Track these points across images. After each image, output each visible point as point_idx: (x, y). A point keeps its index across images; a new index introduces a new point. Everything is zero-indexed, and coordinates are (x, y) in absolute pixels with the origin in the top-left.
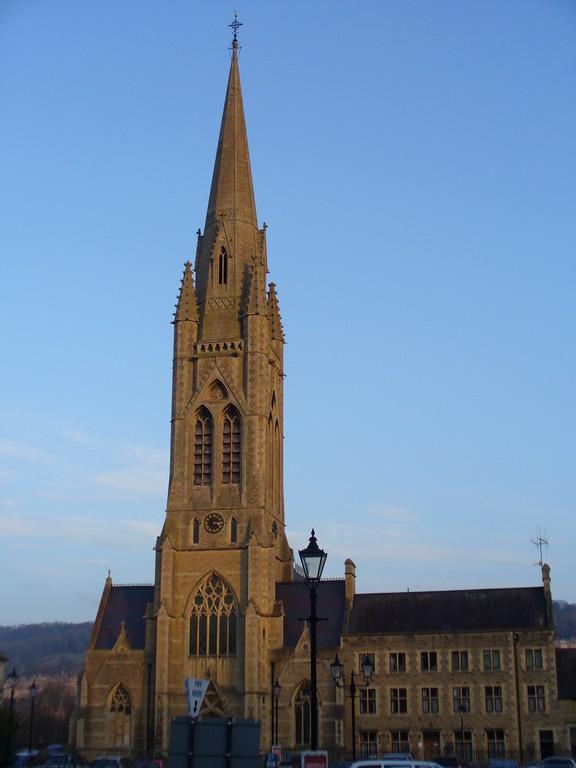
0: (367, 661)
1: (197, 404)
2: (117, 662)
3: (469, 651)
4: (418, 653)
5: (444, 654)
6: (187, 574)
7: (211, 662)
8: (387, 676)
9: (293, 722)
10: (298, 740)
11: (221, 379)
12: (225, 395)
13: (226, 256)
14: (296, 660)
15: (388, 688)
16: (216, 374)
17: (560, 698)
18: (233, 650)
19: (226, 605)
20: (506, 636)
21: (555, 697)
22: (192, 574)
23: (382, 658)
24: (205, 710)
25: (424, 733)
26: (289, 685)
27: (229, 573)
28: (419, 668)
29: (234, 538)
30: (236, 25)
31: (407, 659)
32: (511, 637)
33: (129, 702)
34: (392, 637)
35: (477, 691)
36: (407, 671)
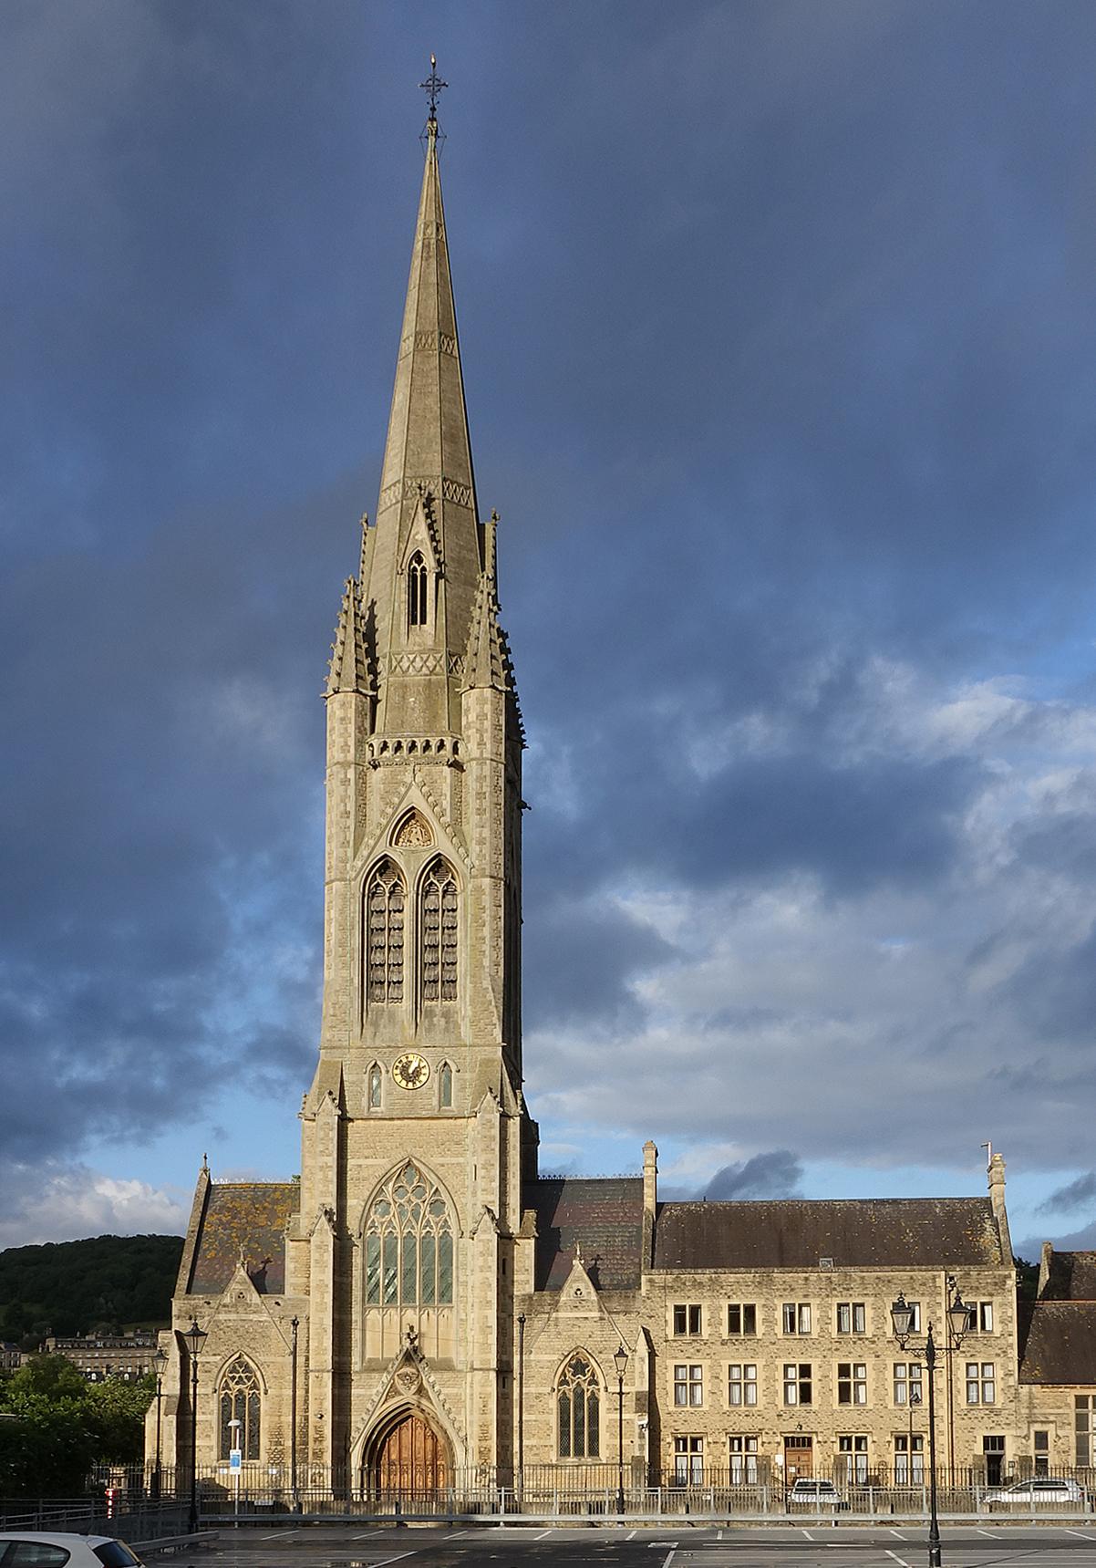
0: (687, 1320)
1: (378, 853)
2: (233, 1316)
3: (869, 1301)
4: (779, 1303)
5: (824, 1308)
6: (361, 1162)
7: (411, 1316)
8: (724, 1343)
9: (553, 1420)
10: (564, 1452)
11: (422, 807)
12: (427, 835)
13: (424, 569)
14: (560, 1315)
15: (725, 1364)
16: (416, 799)
17: (1021, 1382)
18: (446, 1295)
19: (431, 1217)
20: (934, 1278)
21: (1013, 1380)
22: (370, 1161)
23: (715, 1310)
24: (394, 1402)
25: (786, 1439)
26: (547, 1357)
27: (442, 1160)
28: (779, 1329)
29: (445, 1098)
30: (435, 85)
31: (759, 1315)
32: (941, 1282)
33: (255, 1387)
34: (732, 1278)
35: (880, 1371)
36: (759, 1336)
